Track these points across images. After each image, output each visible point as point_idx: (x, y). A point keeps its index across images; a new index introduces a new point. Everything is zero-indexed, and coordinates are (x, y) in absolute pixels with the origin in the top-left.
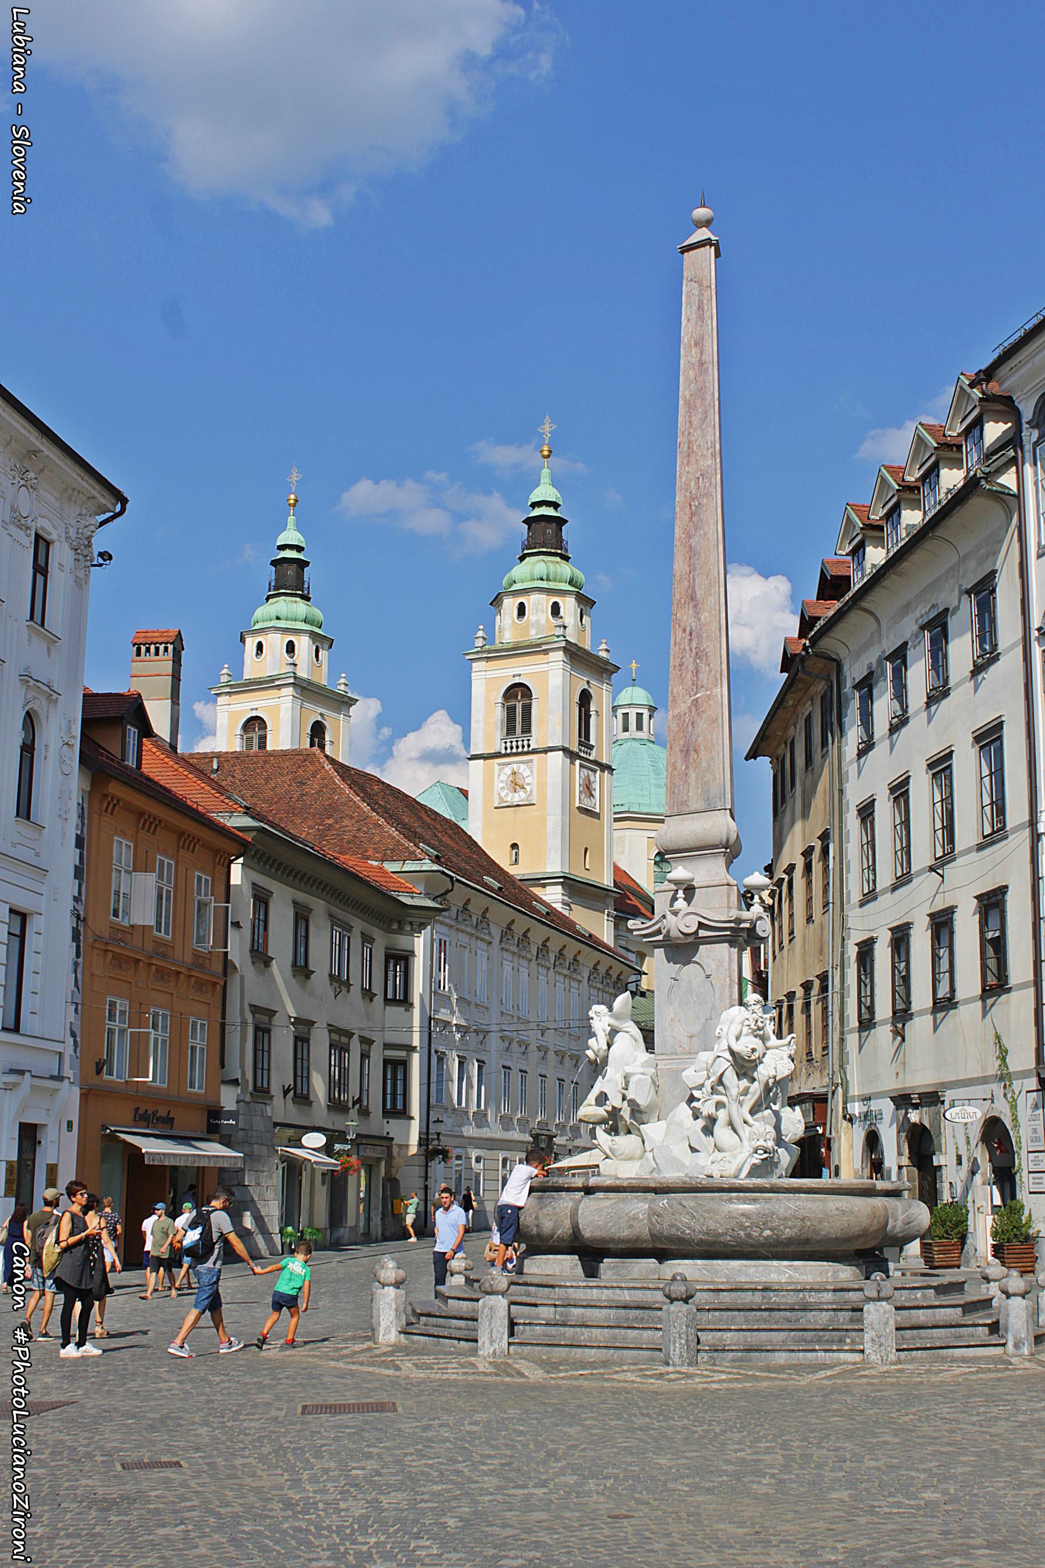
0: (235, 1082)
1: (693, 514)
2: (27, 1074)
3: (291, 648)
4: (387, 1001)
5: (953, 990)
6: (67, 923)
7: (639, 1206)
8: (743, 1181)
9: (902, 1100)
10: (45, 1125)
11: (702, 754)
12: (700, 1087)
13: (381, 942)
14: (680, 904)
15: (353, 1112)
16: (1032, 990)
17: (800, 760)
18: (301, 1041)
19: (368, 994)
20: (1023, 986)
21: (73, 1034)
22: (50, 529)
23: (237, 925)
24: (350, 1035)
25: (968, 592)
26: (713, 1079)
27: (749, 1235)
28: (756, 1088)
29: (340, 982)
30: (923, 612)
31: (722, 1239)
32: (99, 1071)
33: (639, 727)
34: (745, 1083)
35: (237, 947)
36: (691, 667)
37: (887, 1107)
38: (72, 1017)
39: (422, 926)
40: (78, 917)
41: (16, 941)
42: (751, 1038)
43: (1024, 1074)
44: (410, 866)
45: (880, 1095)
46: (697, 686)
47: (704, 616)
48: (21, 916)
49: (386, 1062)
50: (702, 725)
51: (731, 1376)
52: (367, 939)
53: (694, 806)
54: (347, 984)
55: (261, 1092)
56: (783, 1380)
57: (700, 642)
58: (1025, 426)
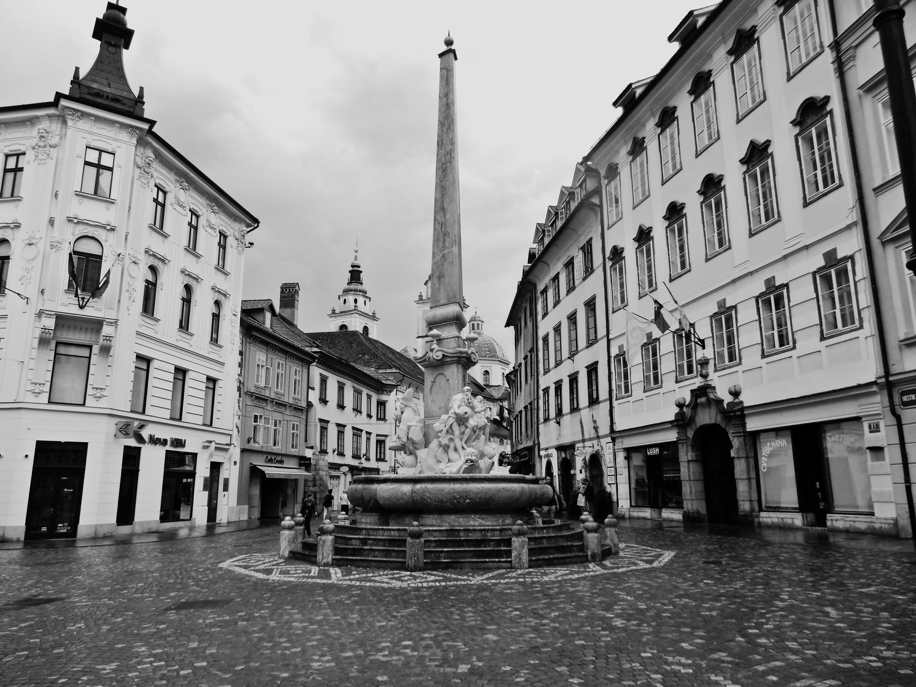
0: (312, 448)
1: (444, 171)
2: (213, 443)
3: (356, 301)
4: (378, 419)
5: (578, 404)
6: (236, 384)
7: (407, 488)
8: (461, 475)
9: (560, 448)
10: (223, 463)
11: (446, 278)
12: (441, 431)
13: (375, 398)
14: (435, 346)
15: (363, 460)
16: (608, 402)
17: (523, 325)
18: (341, 433)
19: (369, 416)
20: (604, 401)
21: (237, 427)
22: (226, 231)
23: (313, 389)
24: (361, 431)
25: (581, 248)
26: (447, 427)
27: (459, 502)
28: (468, 431)
29: (357, 410)
30: (565, 259)
31: (446, 504)
32: (249, 442)
33: (478, 328)
34: (463, 428)
35: (314, 396)
36: (442, 240)
37: (554, 452)
38: (236, 420)
39: (391, 391)
40: (240, 382)
41: (211, 391)
42: (465, 407)
43: (605, 436)
44: (388, 371)
45: (551, 448)
46: (444, 248)
47: (448, 216)
48: (212, 381)
49: (377, 441)
50: (446, 265)
51: (437, 578)
52: (369, 397)
53: (442, 302)
54: (361, 412)
55: (324, 452)
56: (464, 580)
57: (446, 228)
58: (602, 179)
